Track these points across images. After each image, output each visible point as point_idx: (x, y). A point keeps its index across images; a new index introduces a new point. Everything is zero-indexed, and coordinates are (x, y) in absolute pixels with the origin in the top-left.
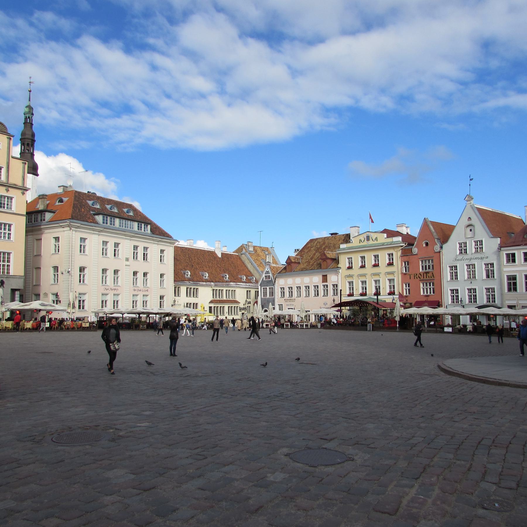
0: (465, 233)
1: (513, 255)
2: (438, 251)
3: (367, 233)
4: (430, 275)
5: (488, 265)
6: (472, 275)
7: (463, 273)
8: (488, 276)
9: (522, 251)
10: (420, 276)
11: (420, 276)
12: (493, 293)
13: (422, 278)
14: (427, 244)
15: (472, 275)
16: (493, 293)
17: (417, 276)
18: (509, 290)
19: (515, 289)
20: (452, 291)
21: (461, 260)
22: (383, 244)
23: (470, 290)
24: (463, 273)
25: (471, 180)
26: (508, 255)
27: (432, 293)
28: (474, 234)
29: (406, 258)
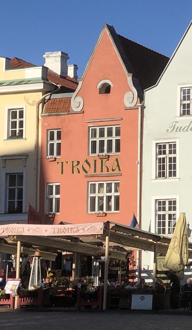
2: (132, 105)
4: (110, 164)
10: (86, 167)
11: (86, 167)
13: (91, 171)
14: (106, 89)
20: (161, 204)
27: (113, 210)
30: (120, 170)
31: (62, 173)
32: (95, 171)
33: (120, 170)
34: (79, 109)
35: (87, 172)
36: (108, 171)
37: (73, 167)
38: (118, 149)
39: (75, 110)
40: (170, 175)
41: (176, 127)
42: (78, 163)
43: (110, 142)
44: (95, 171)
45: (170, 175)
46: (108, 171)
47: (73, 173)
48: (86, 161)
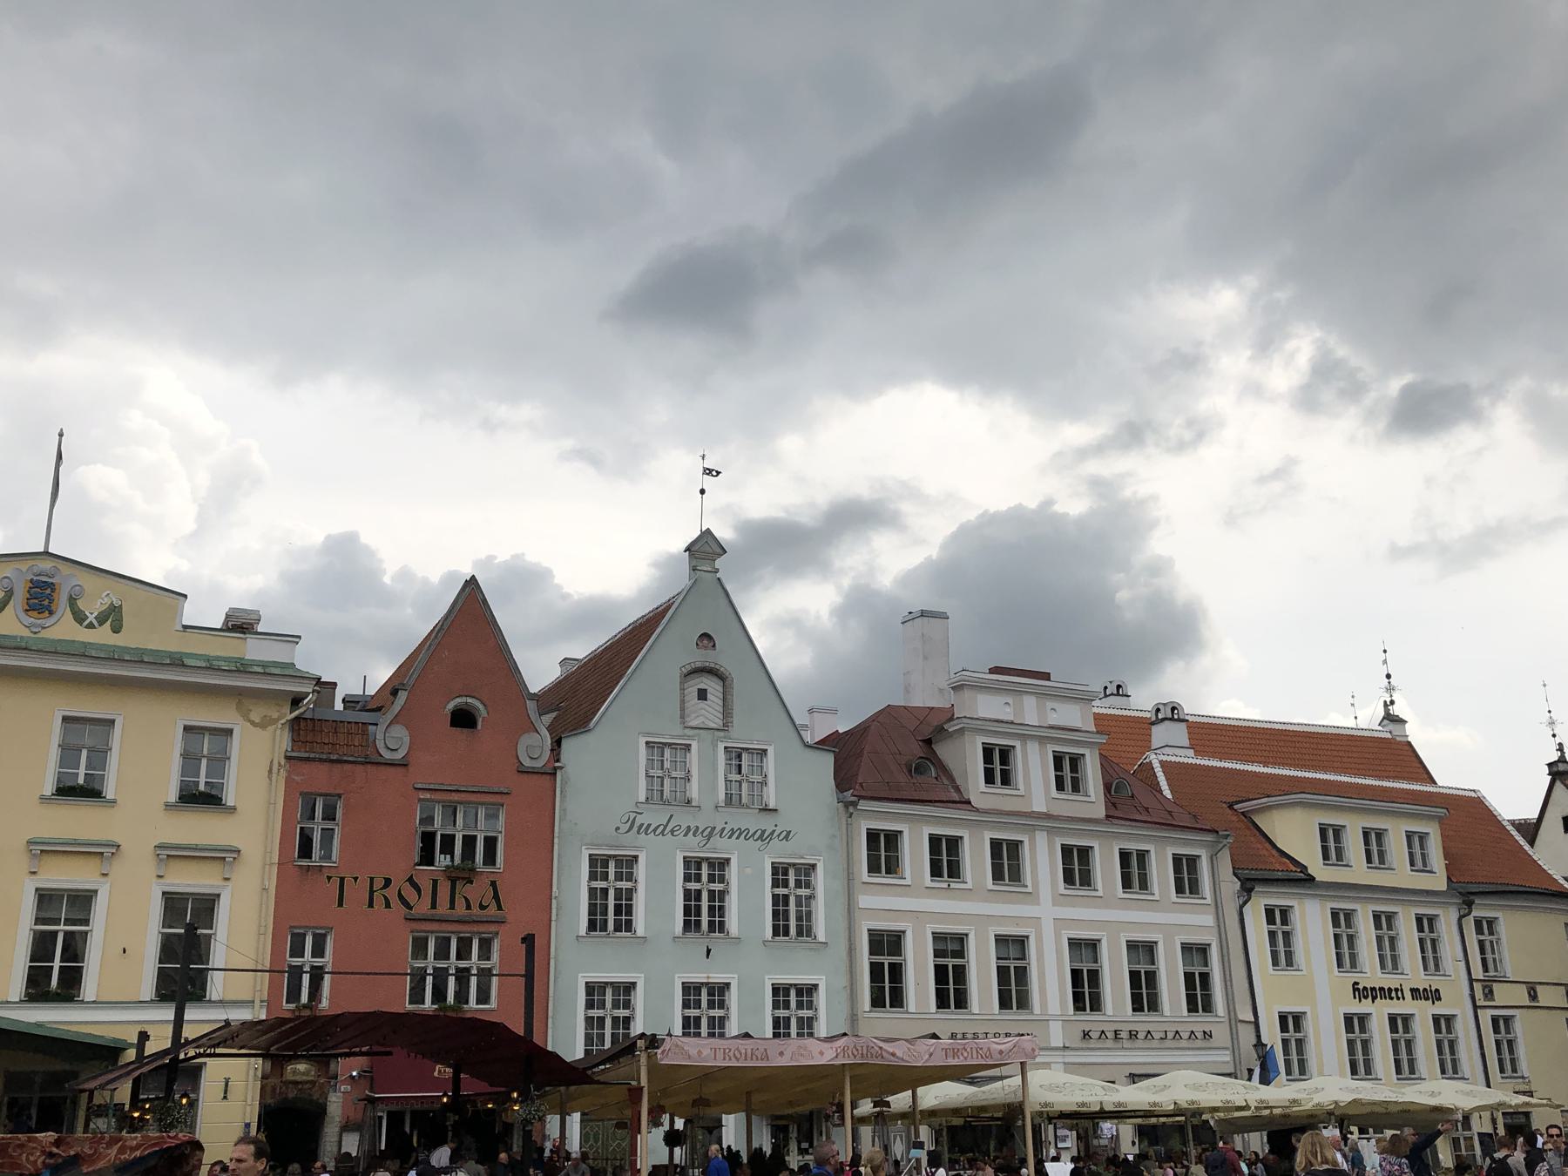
0: (683, 702)
1: (893, 839)
2: (539, 764)
3: (47, 565)
4: (477, 891)
5: (786, 873)
6: (703, 913)
7: (658, 900)
8: (780, 930)
9: (928, 830)
12: (782, 1013)
13: (422, 907)
14: (463, 719)
15: (703, 913)
16: (782, 1013)
17: (392, 893)
18: (877, 1002)
19: (898, 1000)
21: (661, 831)
22: (177, 661)
23: (691, 990)
24: (658, 900)
25: (708, 472)
26: (873, 836)
28: (727, 712)
29: (320, 777)
30: (500, 908)
31: (340, 904)
32: (434, 906)
33: (500, 908)
34: (399, 755)
35: (410, 908)
36: (469, 907)
37: (372, 892)
38: (490, 857)
39: (387, 755)
40: (617, 929)
41: (637, 824)
42: (388, 882)
43: (469, 842)
44: (434, 906)
45: (617, 929)
46: (469, 907)
47: (371, 905)
48: (410, 880)
